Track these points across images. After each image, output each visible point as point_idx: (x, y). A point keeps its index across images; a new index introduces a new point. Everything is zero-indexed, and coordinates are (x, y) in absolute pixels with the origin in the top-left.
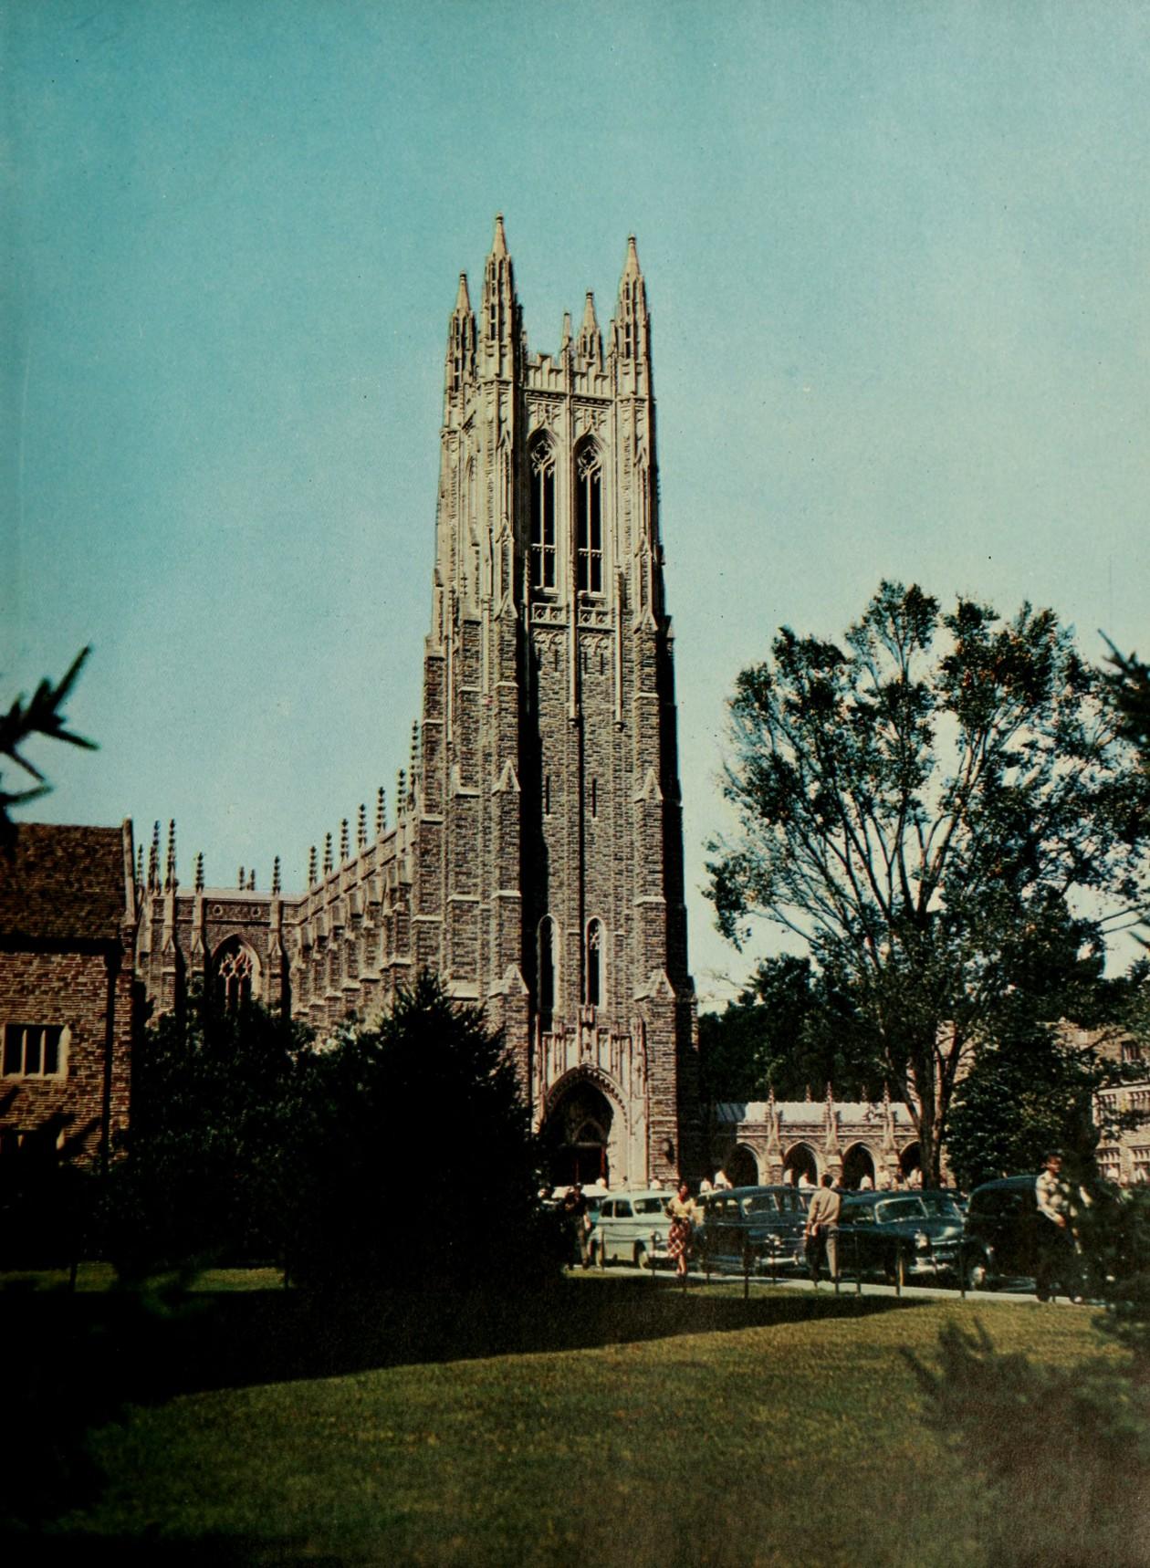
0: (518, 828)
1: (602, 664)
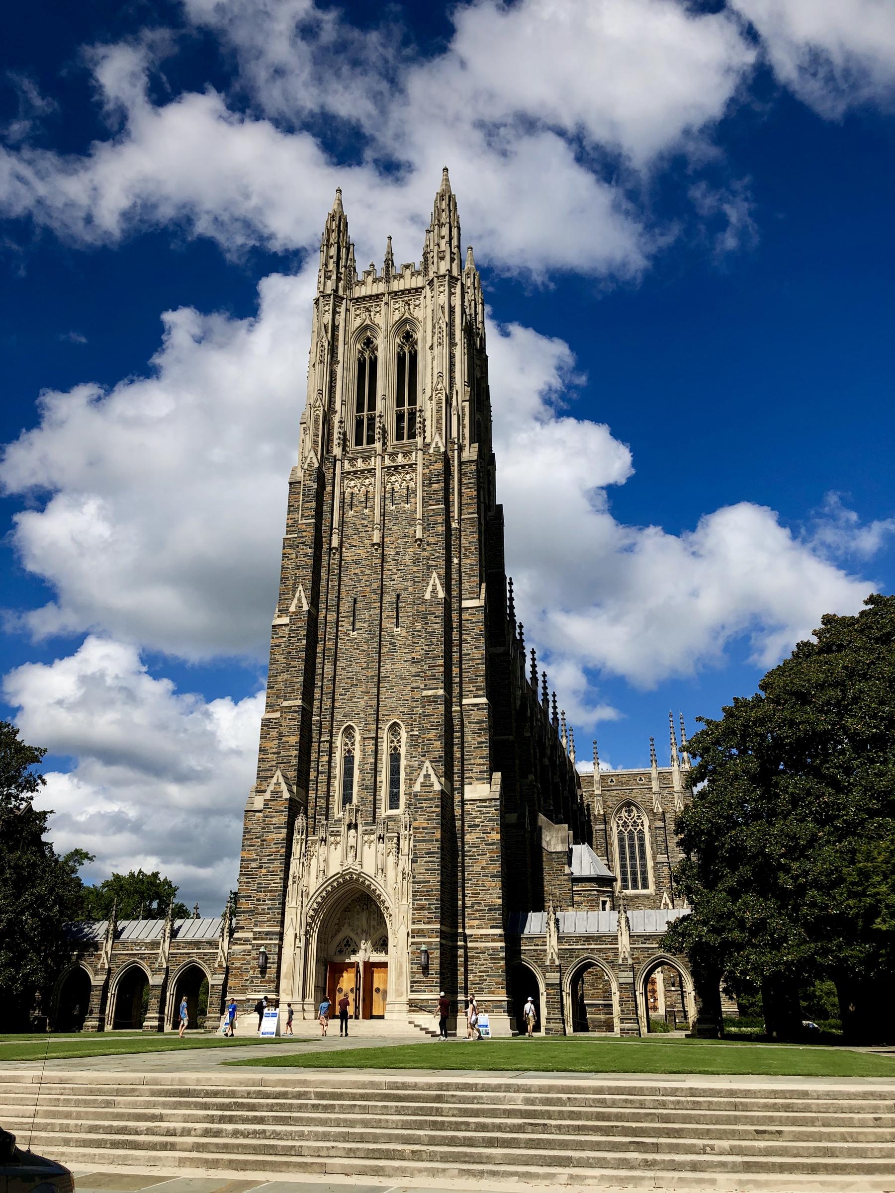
0: (304, 642)
1: (408, 496)
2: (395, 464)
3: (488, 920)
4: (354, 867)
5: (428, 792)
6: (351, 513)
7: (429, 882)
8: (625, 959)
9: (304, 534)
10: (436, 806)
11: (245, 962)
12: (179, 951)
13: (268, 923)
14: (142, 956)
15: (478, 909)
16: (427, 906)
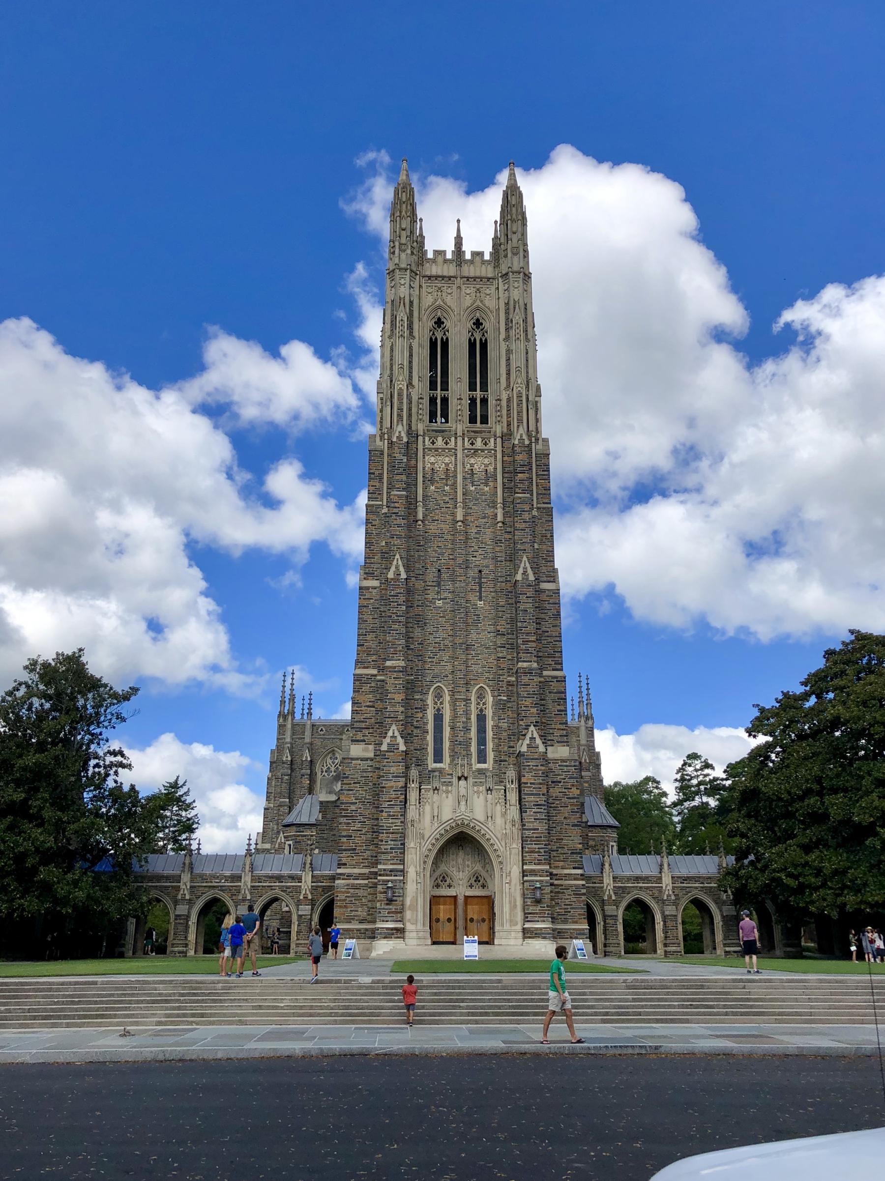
0: (404, 608)
1: (487, 479)
2: (474, 447)
3: (571, 862)
6: (433, 488)
7: (538, 829)
8: (669, 895)
9: (396, 505)
10: (542, 765)
12: (260, 884)
13: (392, 862)
14: (222, 889)
15: (562, 852)
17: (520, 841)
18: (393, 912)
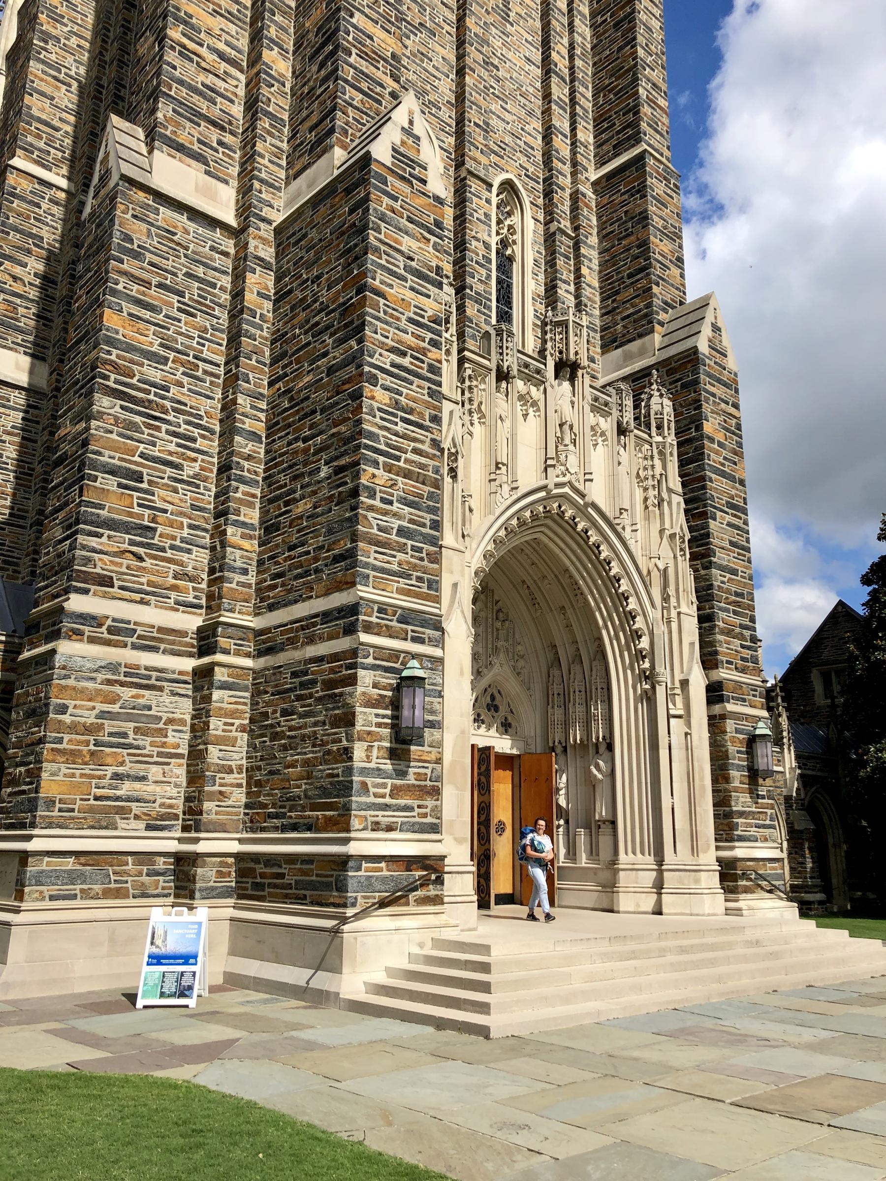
4: (576, 484)
5: (720, 365)
7: (734, 572)
11: (115, 708)
13: (402, 583)
16: (738, 630)
17: (695, 600)
18: (409, 788)
